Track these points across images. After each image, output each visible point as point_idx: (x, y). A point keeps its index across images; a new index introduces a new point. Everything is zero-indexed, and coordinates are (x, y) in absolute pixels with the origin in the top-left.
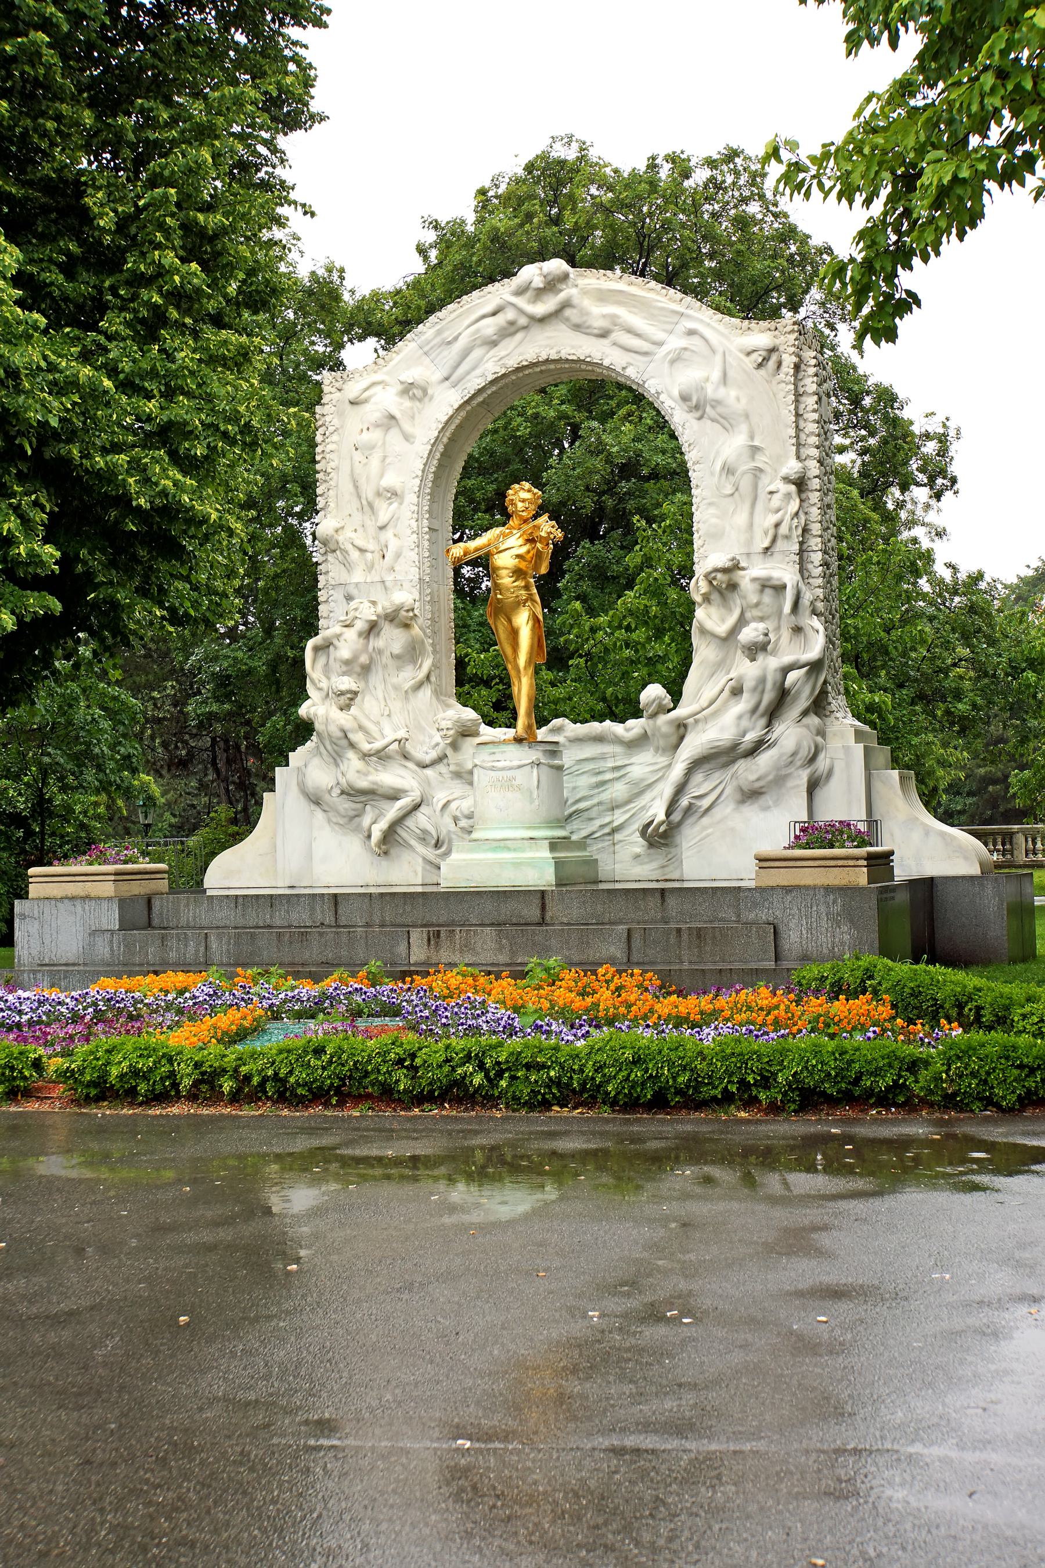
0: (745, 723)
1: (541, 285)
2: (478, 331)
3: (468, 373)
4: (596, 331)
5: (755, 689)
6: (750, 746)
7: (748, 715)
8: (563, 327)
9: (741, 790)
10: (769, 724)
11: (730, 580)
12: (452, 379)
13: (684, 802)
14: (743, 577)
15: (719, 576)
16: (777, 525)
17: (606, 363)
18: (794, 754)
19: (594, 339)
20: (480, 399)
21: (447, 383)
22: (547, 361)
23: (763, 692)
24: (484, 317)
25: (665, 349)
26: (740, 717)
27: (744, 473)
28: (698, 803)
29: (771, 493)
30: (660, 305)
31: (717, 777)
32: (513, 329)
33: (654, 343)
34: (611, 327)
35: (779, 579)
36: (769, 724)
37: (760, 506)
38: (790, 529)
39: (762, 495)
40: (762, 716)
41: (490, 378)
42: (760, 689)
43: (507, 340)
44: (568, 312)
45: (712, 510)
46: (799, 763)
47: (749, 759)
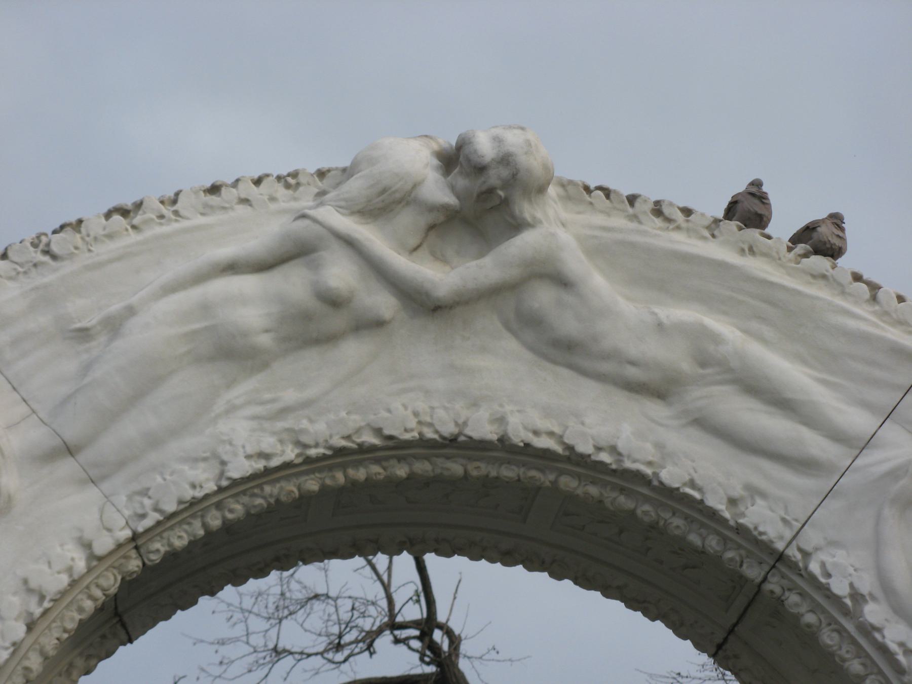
1: (449, 199)
2: (205, 308)
3: (154, 441)
4: (632, 372)
8: (511, 344)
12: (86, 456)
17: (671, 476)
19: (621, 397)
20: (179, 539)
21: (67, 467)
22: (454, 444)
24: (232, 268)
25: (876, 461)
30: (852, 324)
32: (338, 321)
33: (838, 436)
34: (686, 366)
41: (240, 468)
43: (311, 357)
44: (543, 297)
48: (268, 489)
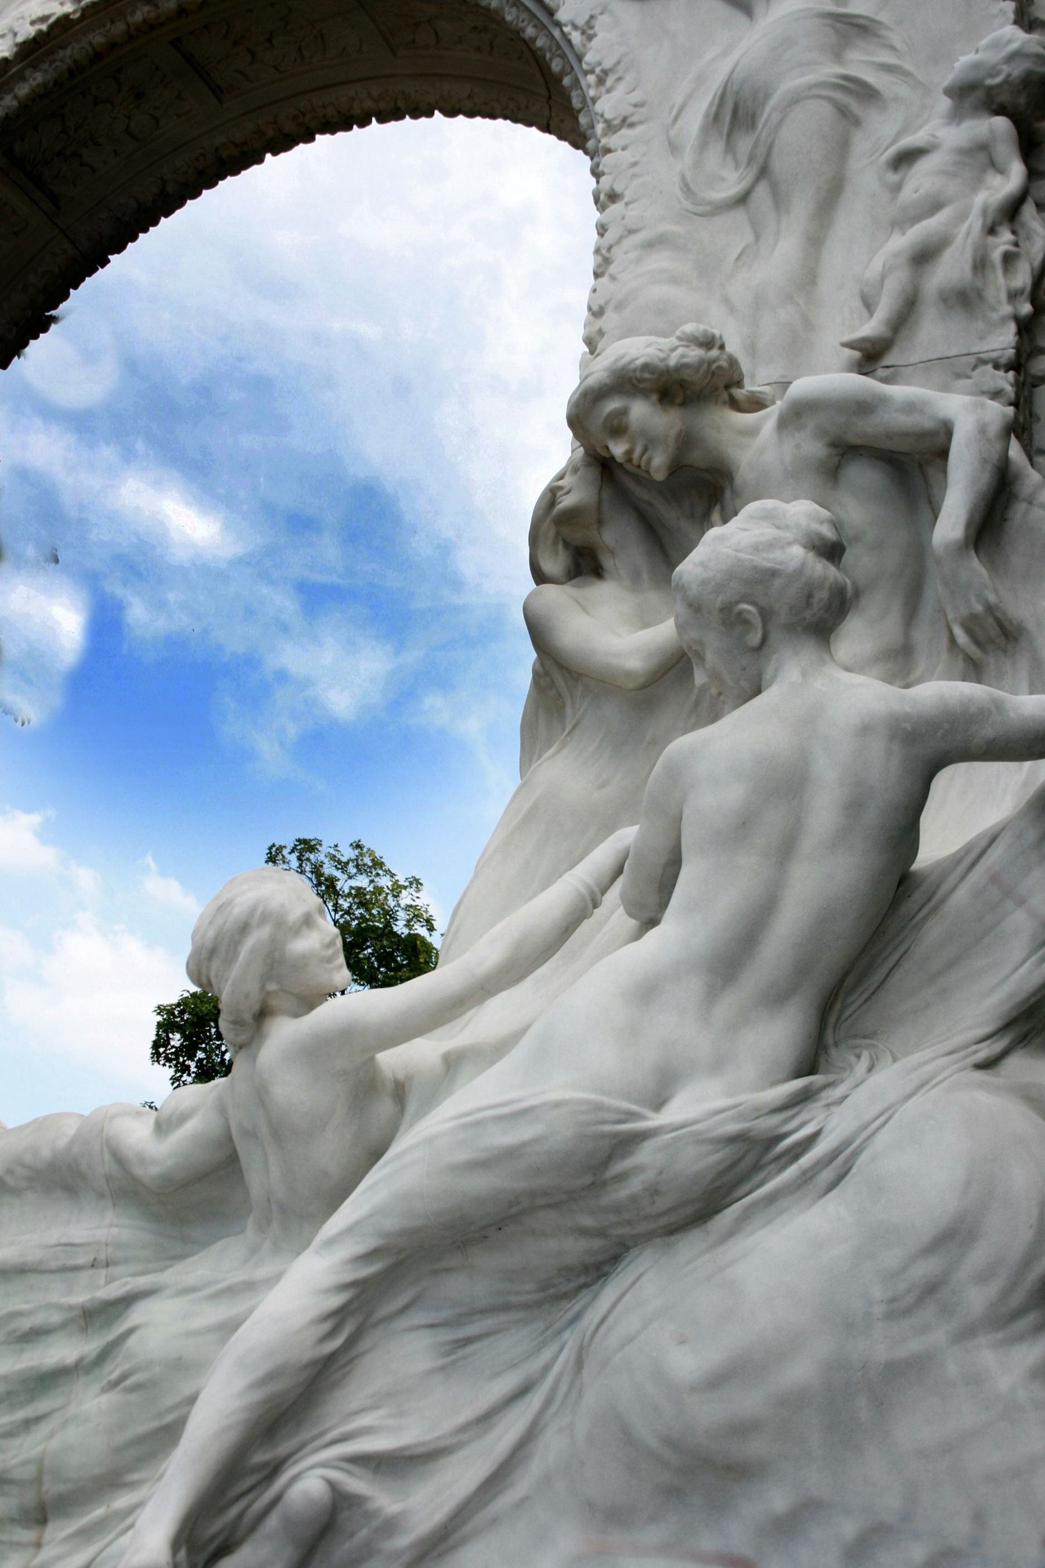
0: (678, 1026)
5: (741, 828)
6: (696, 1162)
7: (693, 987)
9: (626, 1435)
10: (813, 1059)
11: (687, 441)
13: (307, 1482)
14: (752, 432)
15: (641, 411)
16: (924, 257)
18: (954, 1236)
23: (786, 850)
26: (646, 992)
27: (795, 100)
28: (384, 1499)
29: (906, 159)
31: (509, 1354)
35: (911, 407)
36: (813, 1059)
37: (852, 217)
38: (981, 264)
39: (866, 172)
40: (775, 998)
42: (774, 819)
45: (661, 261)
46: (977, 1299)
47: (691, 1243)
48: (61, 53)
